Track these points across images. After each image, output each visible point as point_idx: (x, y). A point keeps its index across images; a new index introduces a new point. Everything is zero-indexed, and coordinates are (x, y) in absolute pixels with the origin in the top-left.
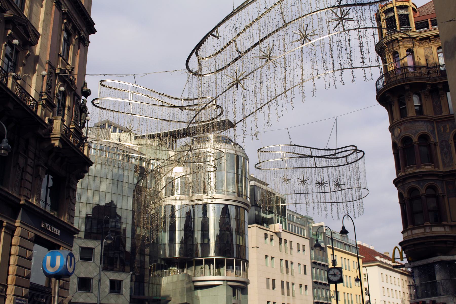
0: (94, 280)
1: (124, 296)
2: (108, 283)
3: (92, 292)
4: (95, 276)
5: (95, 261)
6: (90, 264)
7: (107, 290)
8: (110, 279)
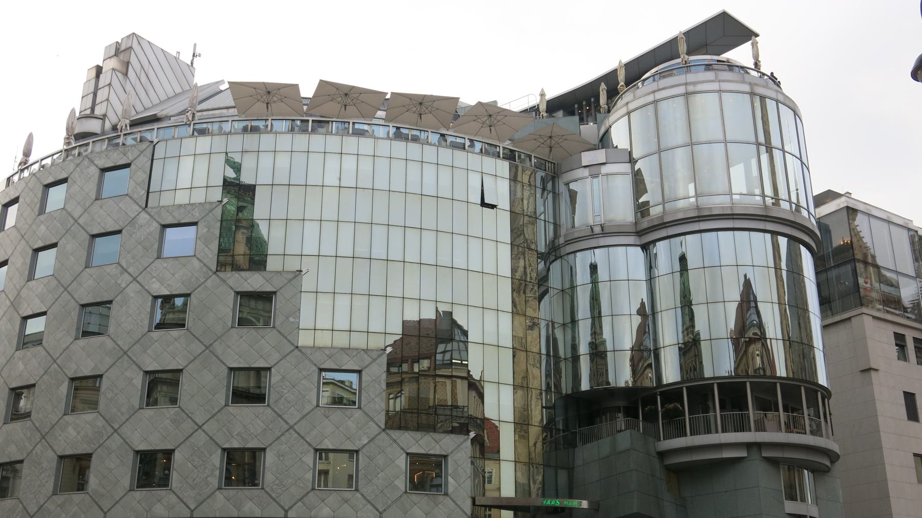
1: (452, 499)
2: (402, 462)
3: (357, 490)
4: (364, 446)
6: (348, 412)
7: (401, 483)
8: (408, 454)
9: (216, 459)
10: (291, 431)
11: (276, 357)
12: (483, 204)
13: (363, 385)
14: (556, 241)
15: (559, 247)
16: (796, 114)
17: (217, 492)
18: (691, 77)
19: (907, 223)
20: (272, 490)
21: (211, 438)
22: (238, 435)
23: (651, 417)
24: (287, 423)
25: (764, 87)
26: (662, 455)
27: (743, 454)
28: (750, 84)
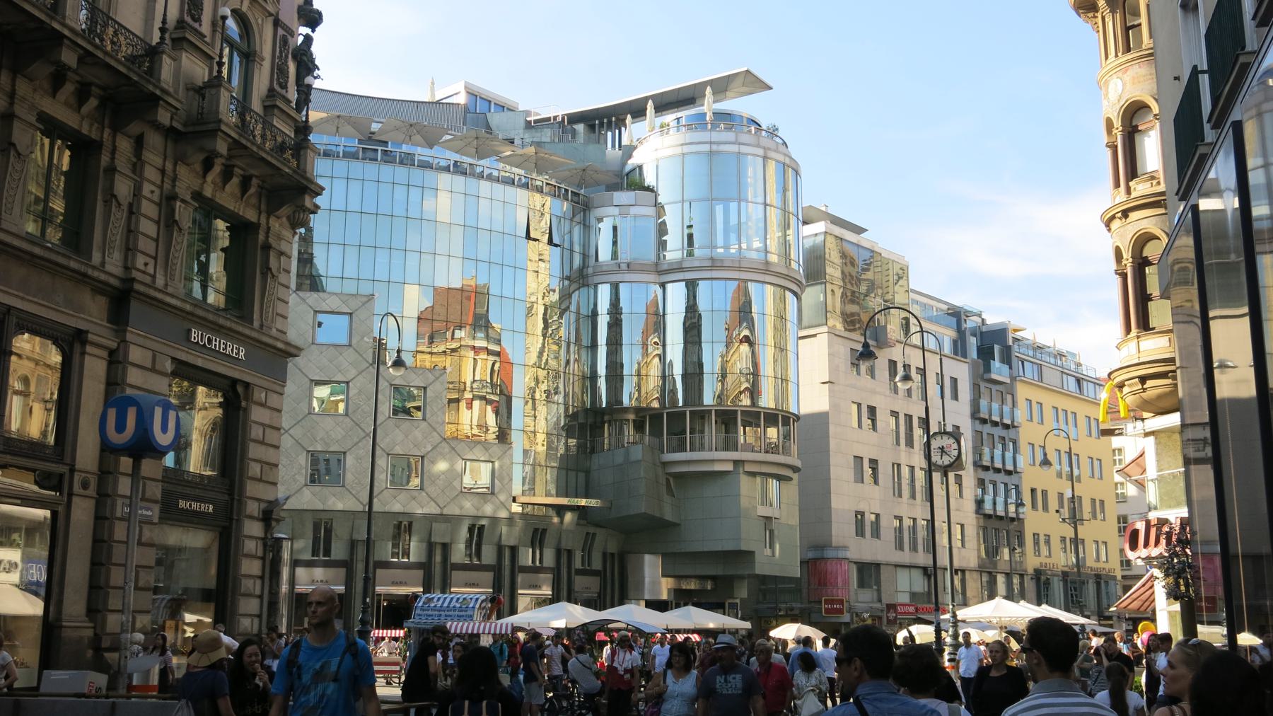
0: (425, 462)
5: (428, 416)
9: (303, 460)
10: (368, 438)
11: (352, 373)
12: (528, 236)
13: (428, 400)
14: (585, 270)
15: (587, 276)
16: (797, 173)
17: (305, 488)
18: (715, 136)
19: (873, 247)
20: (352, 488)
21: (297, 441)
22: (321, 439)
23: (656, 432)
24: (364, 431)
25: (775, 151)
26: (665, 464)
27: (729, 467)
28: (764, 148)
